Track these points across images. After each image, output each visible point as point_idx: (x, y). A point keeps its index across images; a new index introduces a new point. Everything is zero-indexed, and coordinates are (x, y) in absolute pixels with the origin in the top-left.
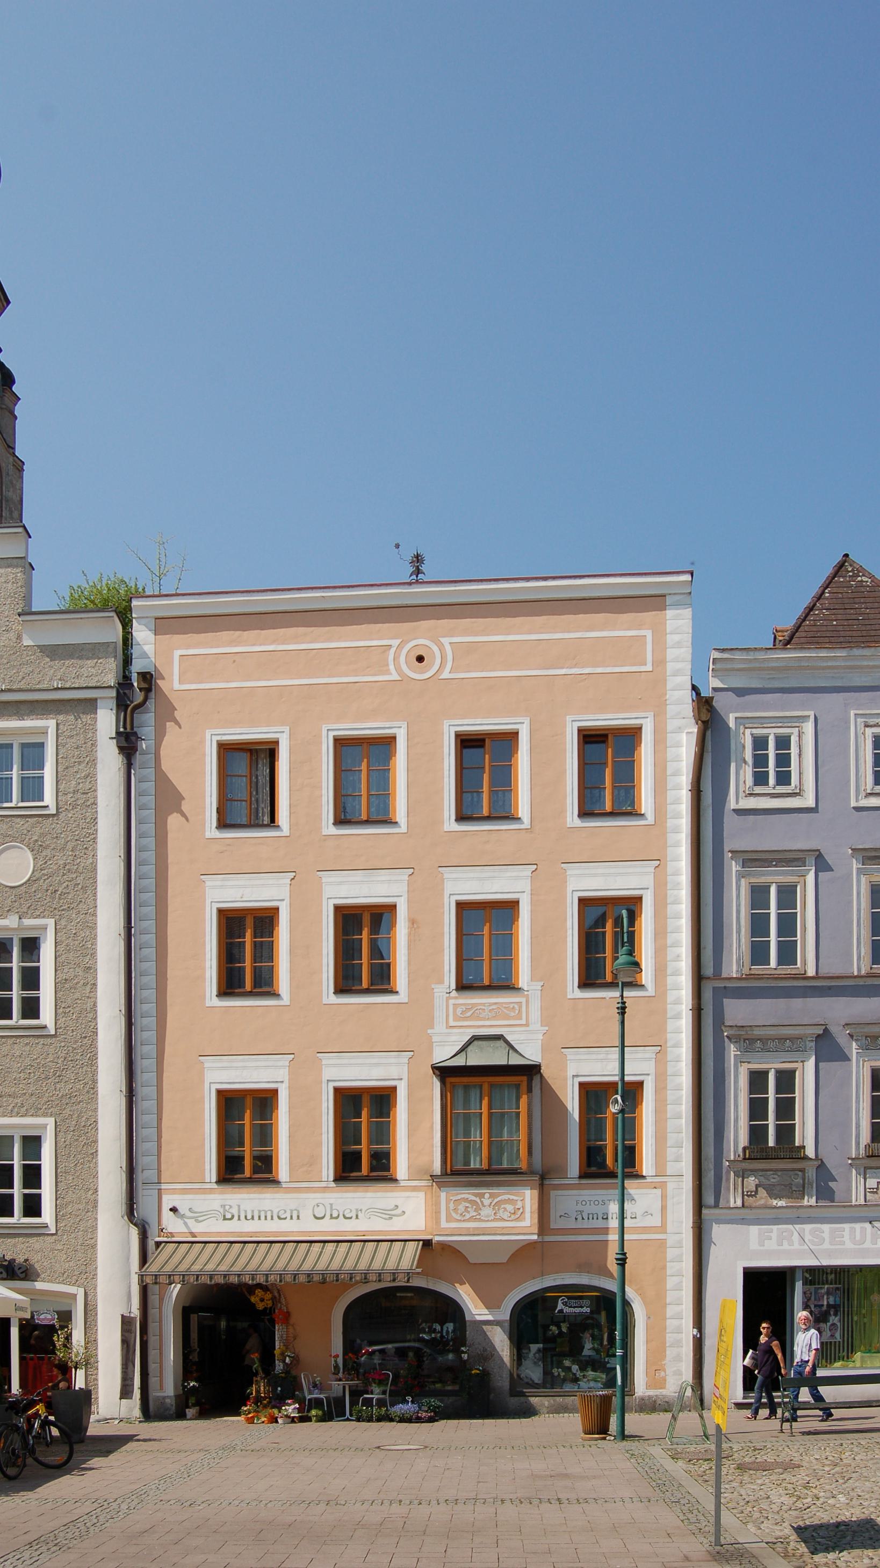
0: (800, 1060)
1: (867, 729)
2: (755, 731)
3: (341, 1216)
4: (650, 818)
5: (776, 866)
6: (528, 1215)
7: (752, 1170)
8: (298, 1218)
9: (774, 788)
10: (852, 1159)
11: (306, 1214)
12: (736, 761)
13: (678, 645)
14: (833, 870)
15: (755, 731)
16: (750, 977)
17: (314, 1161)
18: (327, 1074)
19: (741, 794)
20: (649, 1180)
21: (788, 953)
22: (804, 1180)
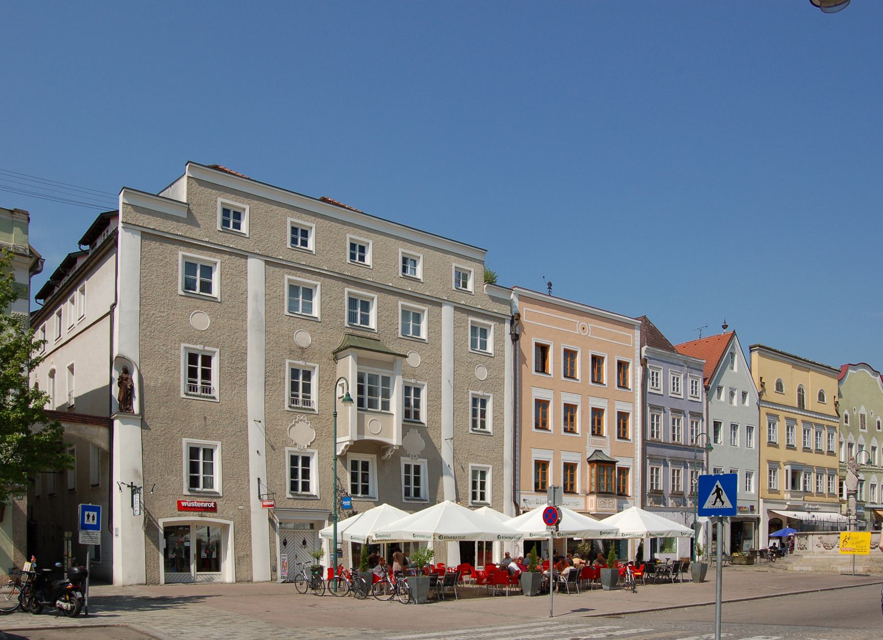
4: (632, 391)
18: (563, 457)
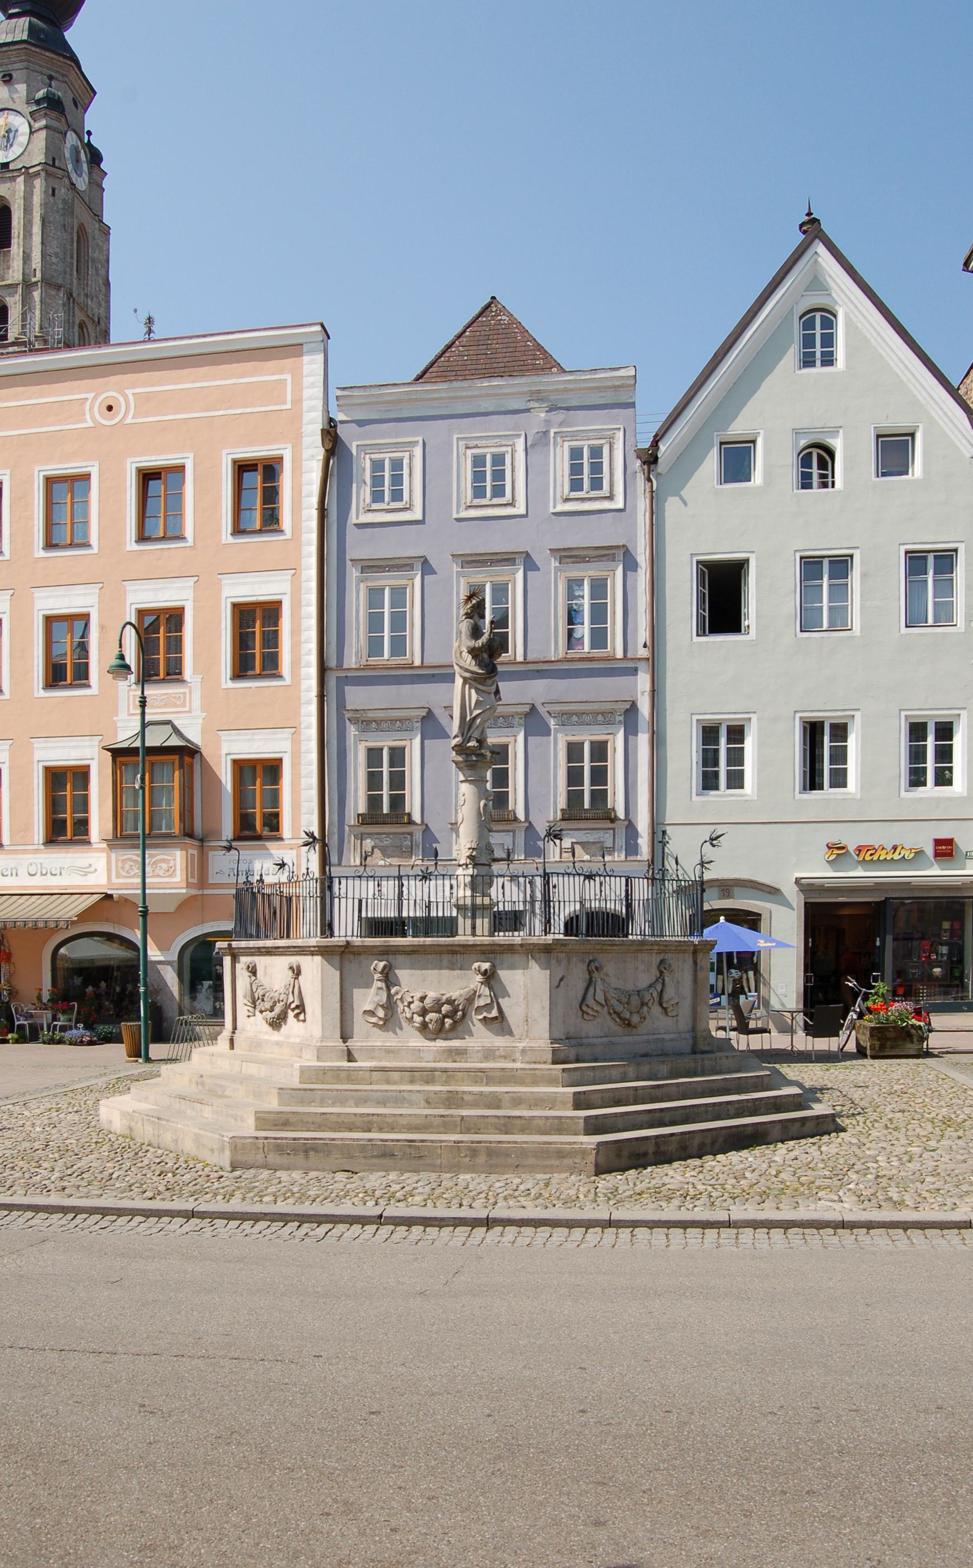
0: (408, 738)
1: (468, 450)
2: (373, 456)
3: (49, 873)
5: (388, 571)
6: (178, 872)
7: (369, 834)
8: (17, 875)
9: (388, 504)
10: (452, 824)
11: (23, 872)
12: (357, 483)
13: (312, 386)
14: (436, 573)
15: (373, 456)
16: (368, 667)
17: (28, 828)
18: (38, 755)
19: (361, 510)
20: (286, 842)
21: (399, 646)
22: (412, 842)
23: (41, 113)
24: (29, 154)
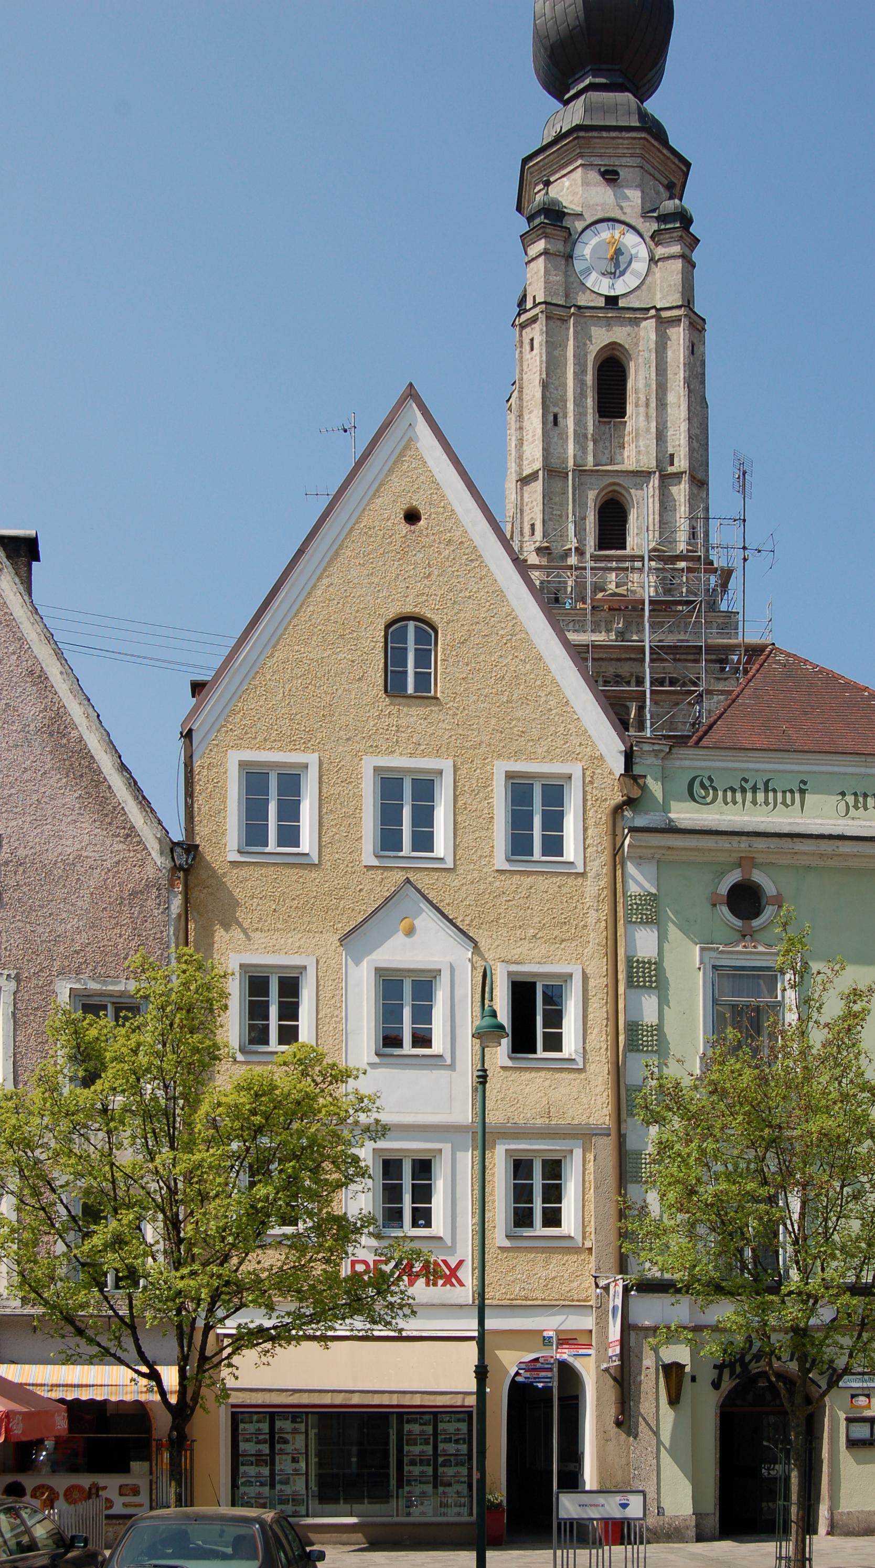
23: (675, 234)
24: (649, 289)
